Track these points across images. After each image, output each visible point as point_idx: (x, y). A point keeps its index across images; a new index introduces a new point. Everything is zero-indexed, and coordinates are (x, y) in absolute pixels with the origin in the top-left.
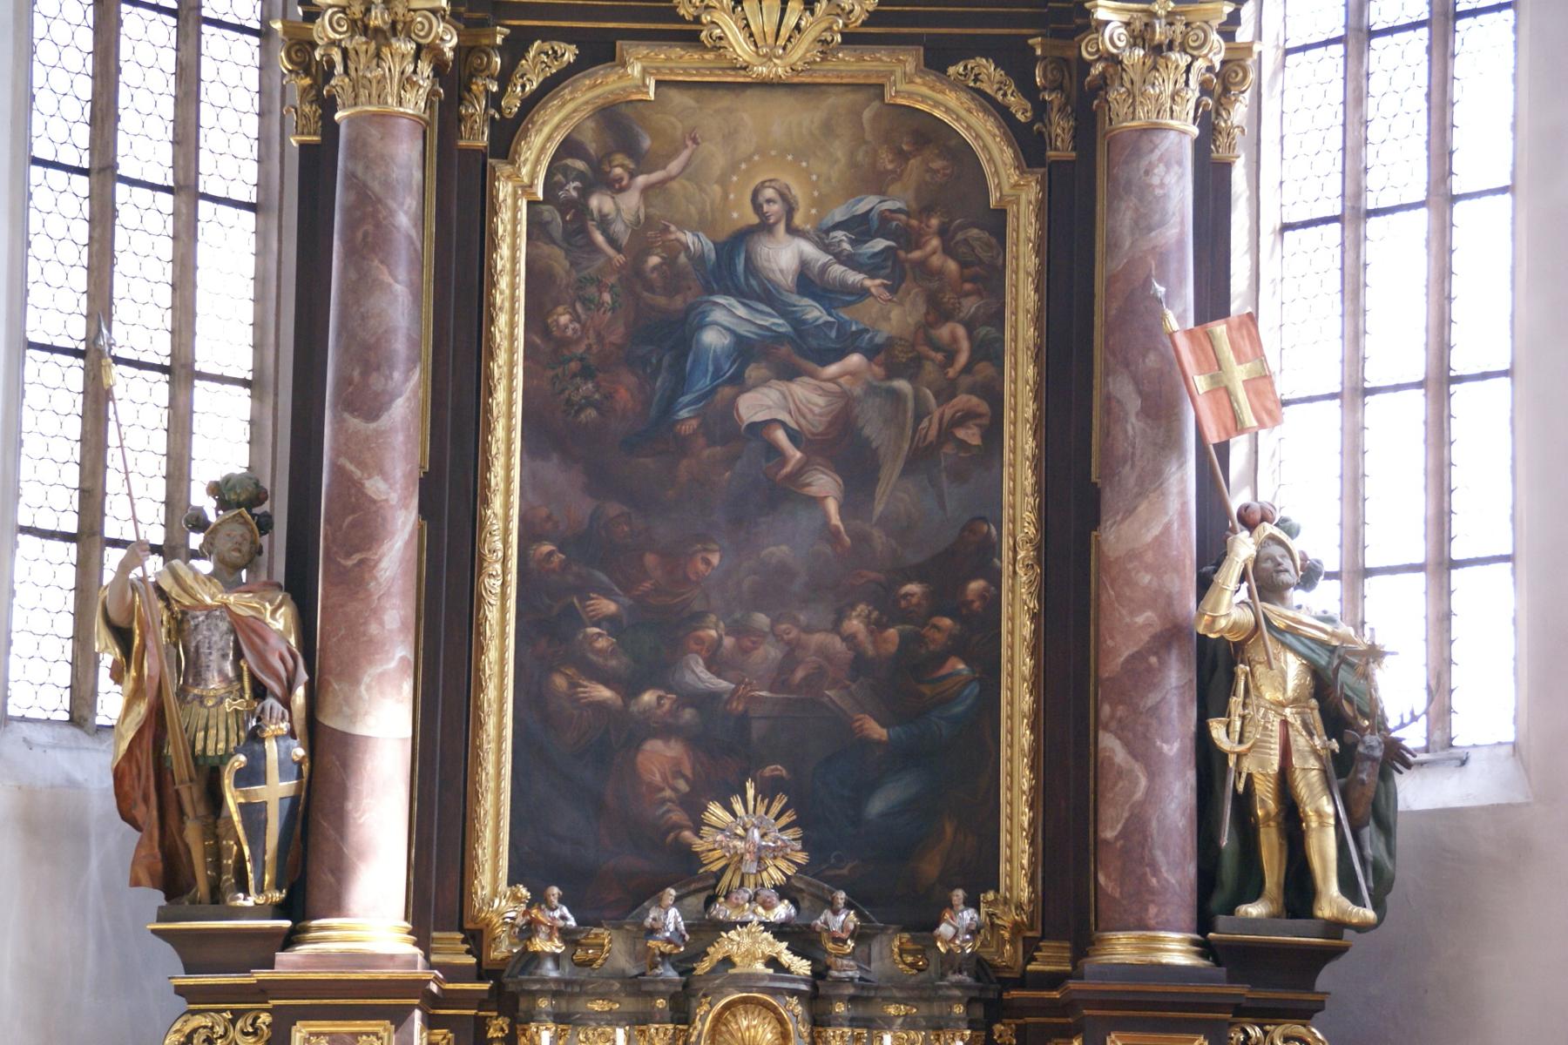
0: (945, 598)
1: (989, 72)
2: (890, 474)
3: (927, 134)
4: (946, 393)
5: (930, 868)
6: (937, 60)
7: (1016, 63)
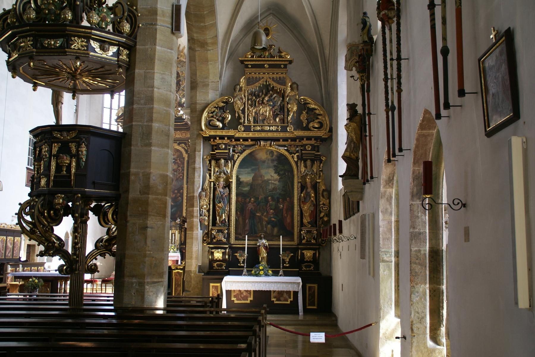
0: (179, 192)
1: (183, 145)
2: (174, 181)
3: (178, 151)
4: (179, 174)
5: (177, 216)
6: (179, 144)
7: (185, 144)
